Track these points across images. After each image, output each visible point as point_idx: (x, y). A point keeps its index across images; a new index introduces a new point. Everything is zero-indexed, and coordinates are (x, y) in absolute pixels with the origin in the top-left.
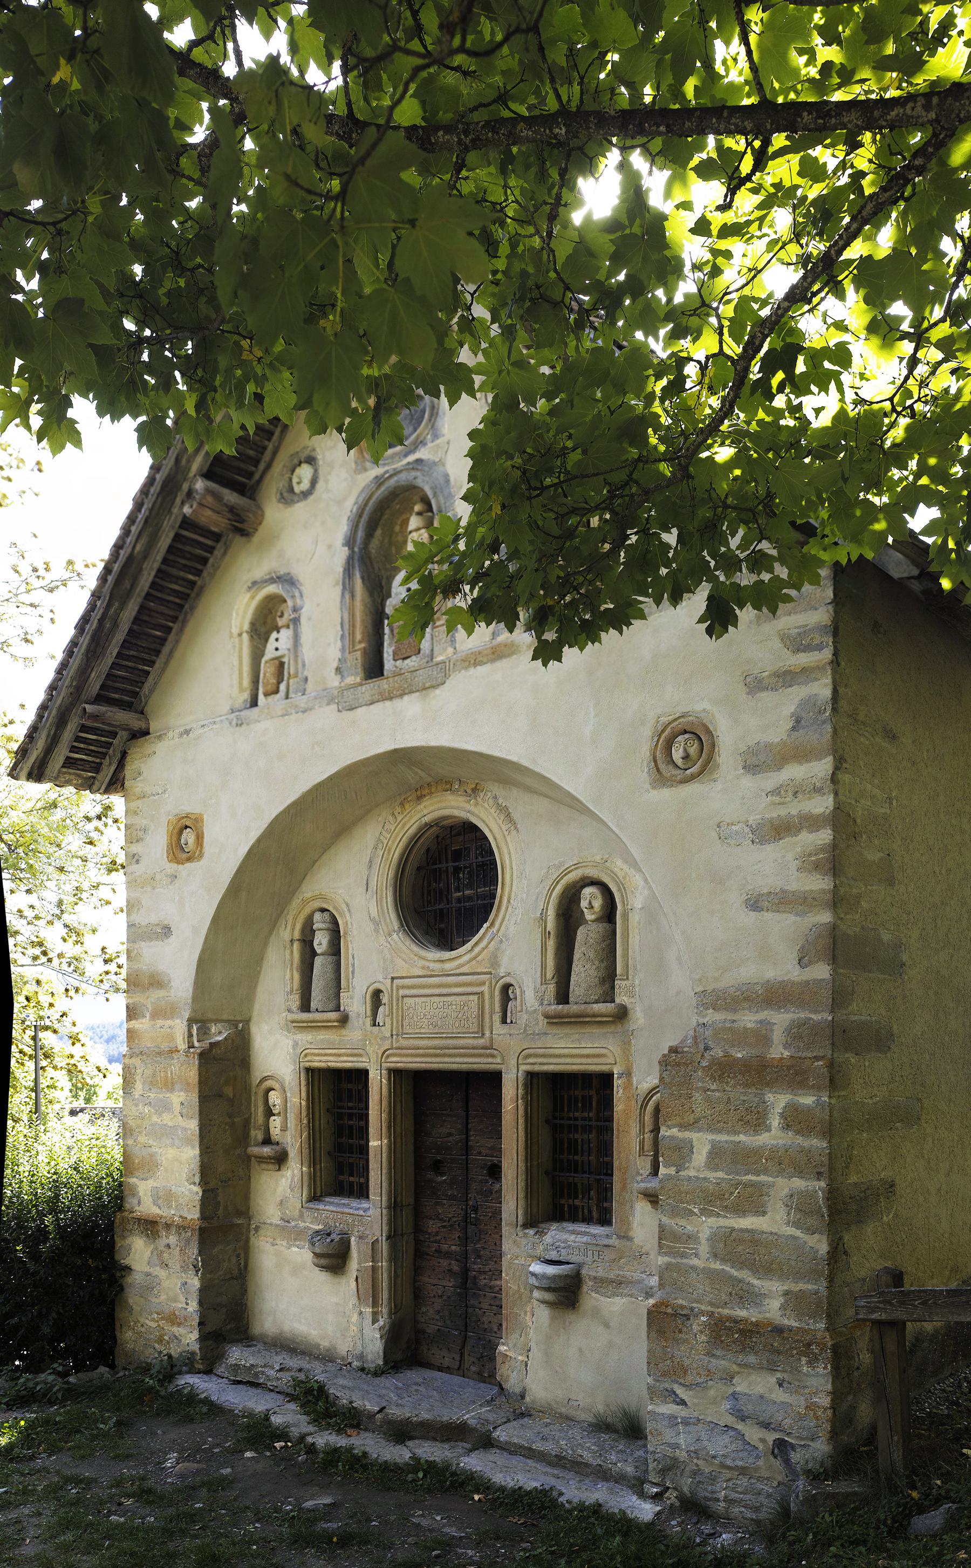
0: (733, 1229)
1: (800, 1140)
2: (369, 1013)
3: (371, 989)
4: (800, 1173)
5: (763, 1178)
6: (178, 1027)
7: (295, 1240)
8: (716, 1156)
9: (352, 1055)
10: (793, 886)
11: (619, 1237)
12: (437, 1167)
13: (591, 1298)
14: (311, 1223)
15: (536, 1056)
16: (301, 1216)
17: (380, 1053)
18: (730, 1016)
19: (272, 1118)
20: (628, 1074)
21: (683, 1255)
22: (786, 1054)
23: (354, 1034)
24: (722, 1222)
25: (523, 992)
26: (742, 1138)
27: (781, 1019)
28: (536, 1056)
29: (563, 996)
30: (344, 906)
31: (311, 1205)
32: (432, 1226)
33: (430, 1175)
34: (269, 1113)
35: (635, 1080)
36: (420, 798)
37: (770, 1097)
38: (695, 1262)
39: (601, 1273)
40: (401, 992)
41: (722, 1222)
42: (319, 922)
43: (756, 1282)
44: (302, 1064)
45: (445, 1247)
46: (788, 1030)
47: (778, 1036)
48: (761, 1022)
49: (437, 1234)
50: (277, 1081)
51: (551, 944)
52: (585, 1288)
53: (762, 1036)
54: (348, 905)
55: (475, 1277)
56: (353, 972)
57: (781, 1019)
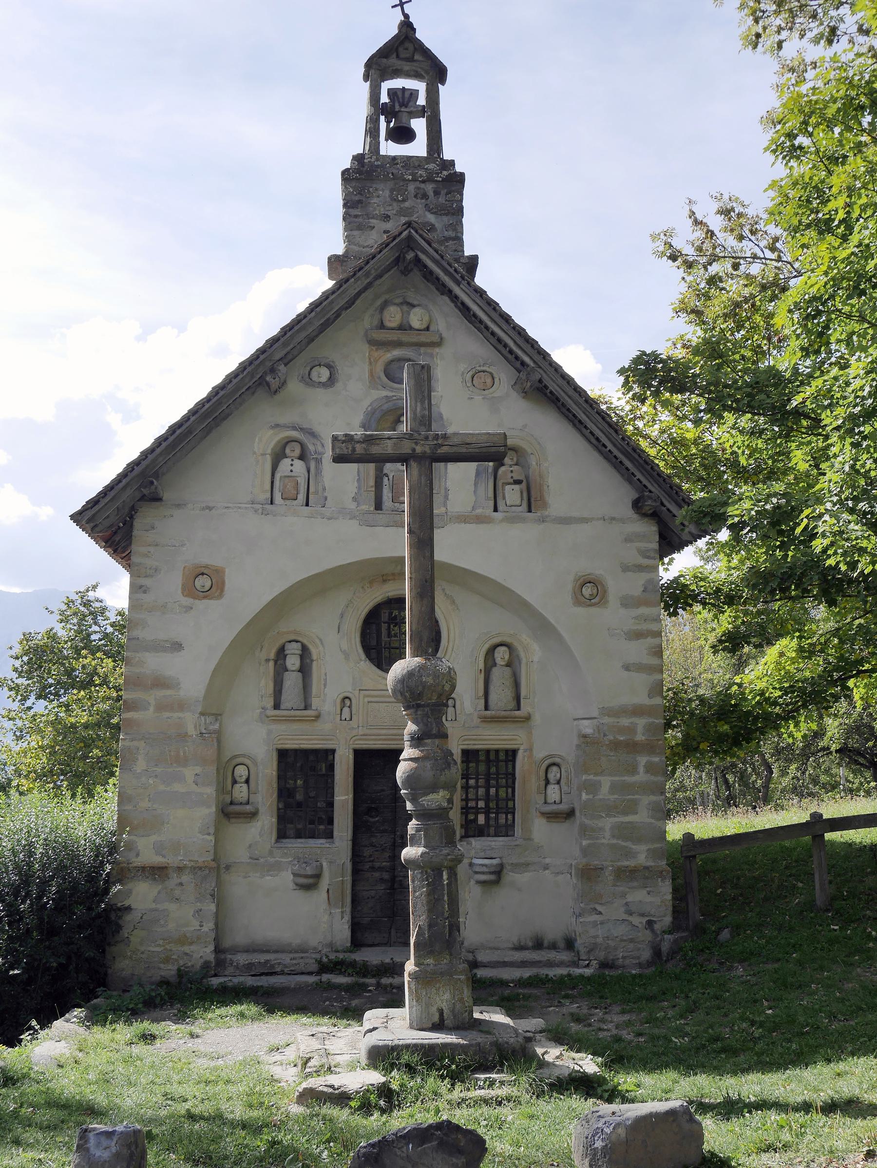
0: (622, 823)
1: (653, 778)
2: (339, 712)
3: (342, 696)
4: (653, 793)
5: (636, 797)
6: (190, 722)
7: (268, 871)
8: (614, 788)
9: (323, 740)
10: (645, 661)
11: (525, 839)
12: (369, 811)
13: (509, 876)
14: (282, 857)
15: (471, 740)
16: (271, 853)
17: (349, 738)
18: (616, 720)
19: (237, 786)
20: (530, 750)
21: (597, 838)
22: (643, 738)
23: (325, 726)
24: (617, 819)
25: (462, 704)
26: (626, 778)
27: (641, 722)
28: (471, 740)
29: (487, 708)
30: (317, 641)
31: (278, 845)
32: (367, 852)
33: (366, 818)
34: (235, 782)
35: (535, 753)
36: (385, 581)
37: (639, 758)
38: (603, 841)
39: (515, 861)
40: (366, 700)
41: (617, 819)
42: (293, 650)
43: (634, 847)
44: (275, 746)
45: (377, 865)
46: (644, 727)
47: (640, 729)
48: (632, 723)
49: (371, 856)
50: (249, 757)
51: (482, 677)
52: (505, 871)
53: (632, 730)
54: (321, 640)
55: (401, 881)
56: (325, 685)
57: (641, 722)
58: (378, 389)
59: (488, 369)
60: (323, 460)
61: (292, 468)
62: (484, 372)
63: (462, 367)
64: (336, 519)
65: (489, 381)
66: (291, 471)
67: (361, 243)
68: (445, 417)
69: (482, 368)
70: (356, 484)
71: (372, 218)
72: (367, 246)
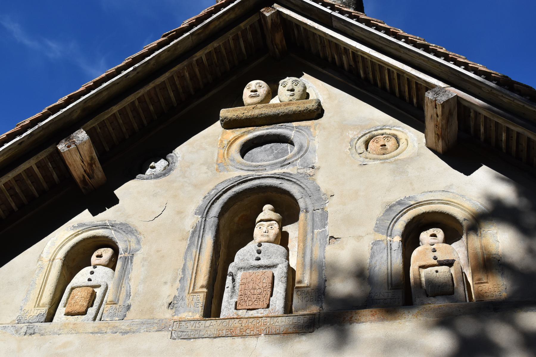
58: (228, 171)
59: (388, 132)
60: (135, 258)
61: (91, 276)
62: (382, 134)
63: (352, 134)
64: (137, 331)
65: (390, 144)
66: (90, 280)
68: (323, 190)
69: (380, 132)
70: (177, 284)
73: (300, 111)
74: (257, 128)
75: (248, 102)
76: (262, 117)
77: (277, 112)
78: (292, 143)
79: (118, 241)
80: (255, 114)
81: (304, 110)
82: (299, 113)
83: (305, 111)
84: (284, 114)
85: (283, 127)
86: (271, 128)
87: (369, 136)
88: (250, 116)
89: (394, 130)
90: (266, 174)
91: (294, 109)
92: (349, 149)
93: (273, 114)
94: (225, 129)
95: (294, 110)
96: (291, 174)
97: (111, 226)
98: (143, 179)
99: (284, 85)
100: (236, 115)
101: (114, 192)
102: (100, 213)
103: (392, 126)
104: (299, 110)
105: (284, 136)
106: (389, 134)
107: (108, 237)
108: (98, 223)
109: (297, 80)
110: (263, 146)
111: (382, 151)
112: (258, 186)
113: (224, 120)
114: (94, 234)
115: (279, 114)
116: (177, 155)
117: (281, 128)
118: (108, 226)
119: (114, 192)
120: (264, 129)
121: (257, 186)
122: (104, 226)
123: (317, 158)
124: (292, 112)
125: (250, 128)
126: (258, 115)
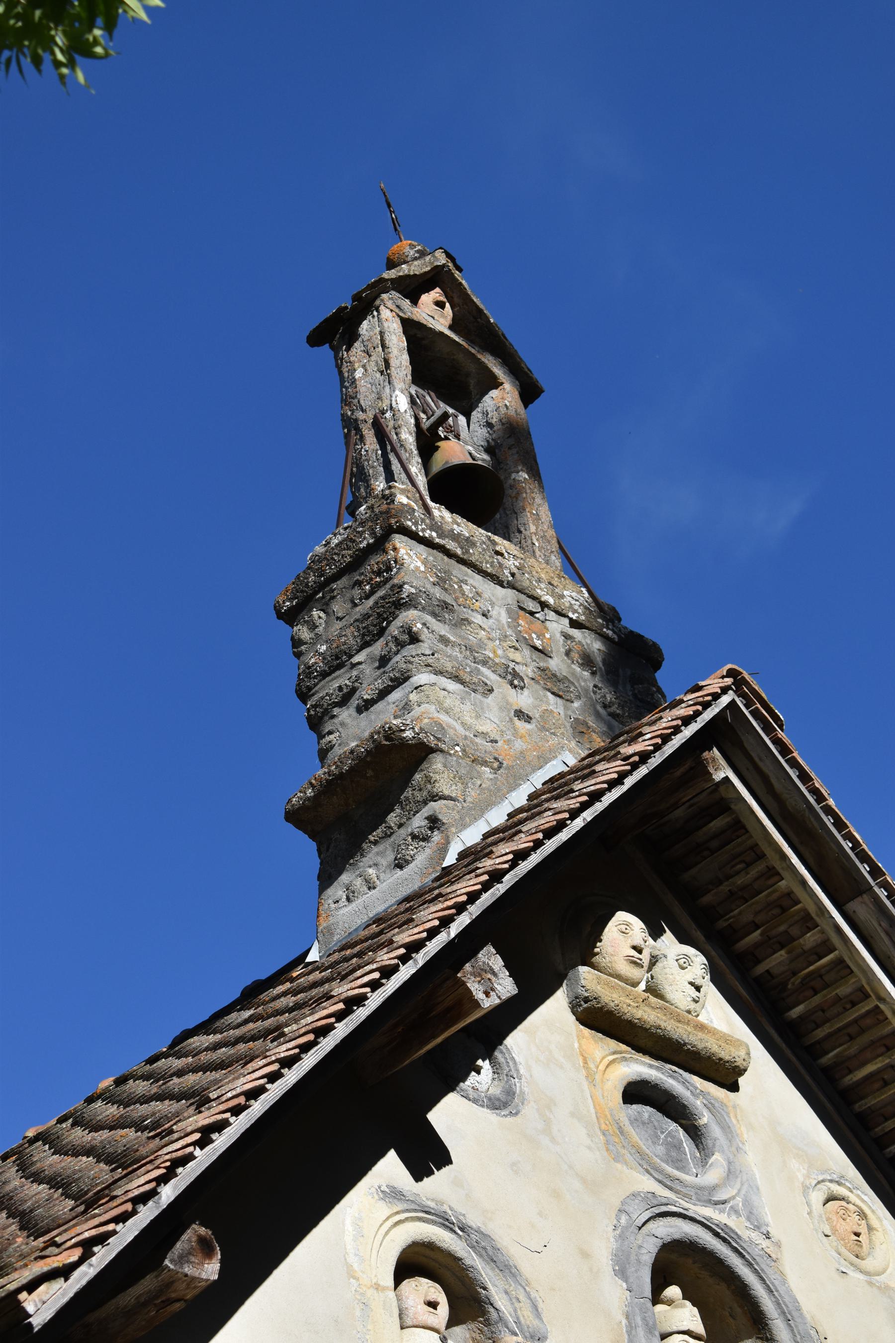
67: (468, 719)
71: (484, 663)
72: (484, 735)
73: (720, 1059)
74: (633, 1052)
75: (618, 969)
76: (656, 1033)
77: (685, 1037)
78: (695, 1132)
79: (490, 1286)
80: (649, 1020)
81: (728, 1062)
82: (716, 1063)
83: (727, 1064)
84: (693, 1051)
85: (674, 1074)
86: (657, 1068)
87: (828, 1193)
88: (638, 1019)
89: (858, 1196)
90: (696, 1212)
91: (714, 1049)
92: (808, 1214)
93: (677, 1040)
94: (577, 1019)
95: (712, 1051)
96: (739, 1237)
97: (460, 1228)
98: (465, 1095)
99: (685, 963)
100: (616, 1002)
101: (432, 1116)
102: (427, 1177)
103: (855, 1185)
104: (720, 1056)
105: (685, 1107)
106: (853, 1202)
107: (460, 1259)
108: (432, 1204)
109: (689, 958)
110: (634, 1106)
111: (856, 1247)
112: (693, 1241)
113: (592, 1001)
114: (434, 1239)
115: (685, 1044)
116: (514, 1055)
117: (674, 1079)
118: (453, 1224)
119: (432, 1116)
120: (644, 1064)
121: (691, 1241)
122: (446, 1223)
123: (768, 1213)
124: (708, 1054)
125: (623, 1047)
126: (653, 1026)
